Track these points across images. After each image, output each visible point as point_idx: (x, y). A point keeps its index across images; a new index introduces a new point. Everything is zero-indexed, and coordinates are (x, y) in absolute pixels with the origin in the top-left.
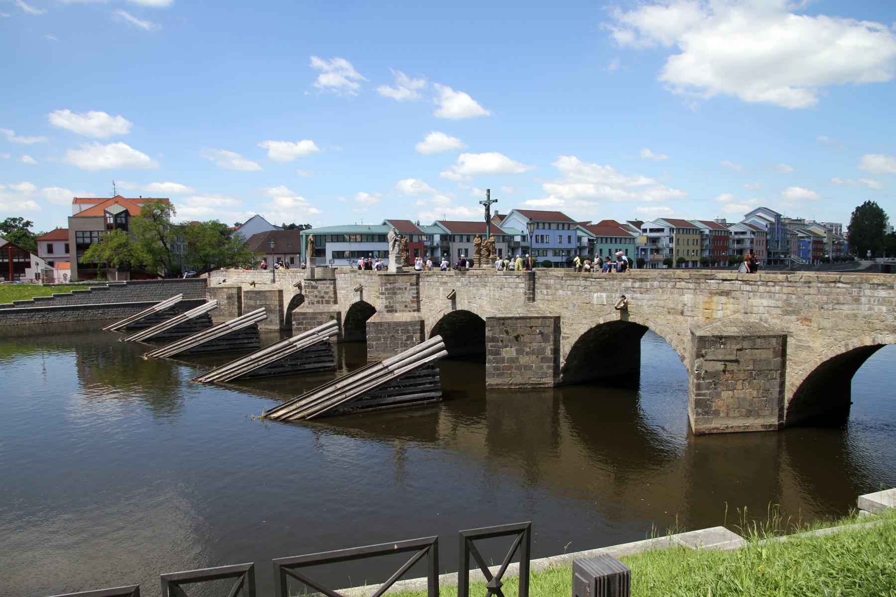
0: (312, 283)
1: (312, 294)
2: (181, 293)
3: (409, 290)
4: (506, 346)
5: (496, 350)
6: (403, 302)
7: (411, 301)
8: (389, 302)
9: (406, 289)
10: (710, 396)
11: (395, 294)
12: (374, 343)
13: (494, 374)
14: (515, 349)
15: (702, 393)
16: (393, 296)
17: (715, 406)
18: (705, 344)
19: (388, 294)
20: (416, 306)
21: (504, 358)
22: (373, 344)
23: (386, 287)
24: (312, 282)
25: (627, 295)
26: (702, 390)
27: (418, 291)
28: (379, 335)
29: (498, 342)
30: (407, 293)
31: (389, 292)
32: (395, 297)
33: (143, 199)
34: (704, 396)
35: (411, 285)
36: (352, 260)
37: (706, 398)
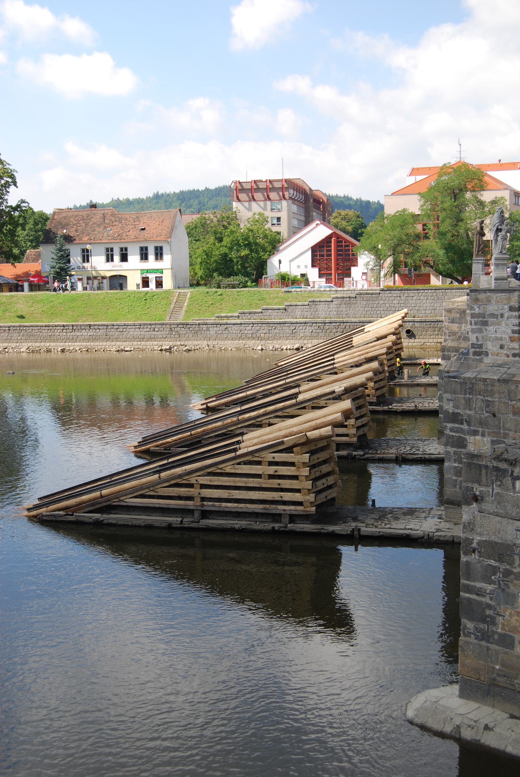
2: (406, 307)
3: (508, 318)
4: (475, 433)
5: (460, 437)
6: (497, 339)
7: (510, 338)
8: (477, 338)
9: (502, 316)
10: (491, 599)
11: (485, 324)
13: (456, 481)
14: (489, 439)
15: (475, 587)
16: (483, 328)
17: (503, 624)
18: (480, 475)
19: (476, 324)
20: (517, 347)
23: (473, 312)
26: (474, 581)
29: (462, 424)
30: (503, 323)
31: (476, 320)
32: (486, 330)
34: (477, 594)
35: (511, 309)
37: (483, 599)
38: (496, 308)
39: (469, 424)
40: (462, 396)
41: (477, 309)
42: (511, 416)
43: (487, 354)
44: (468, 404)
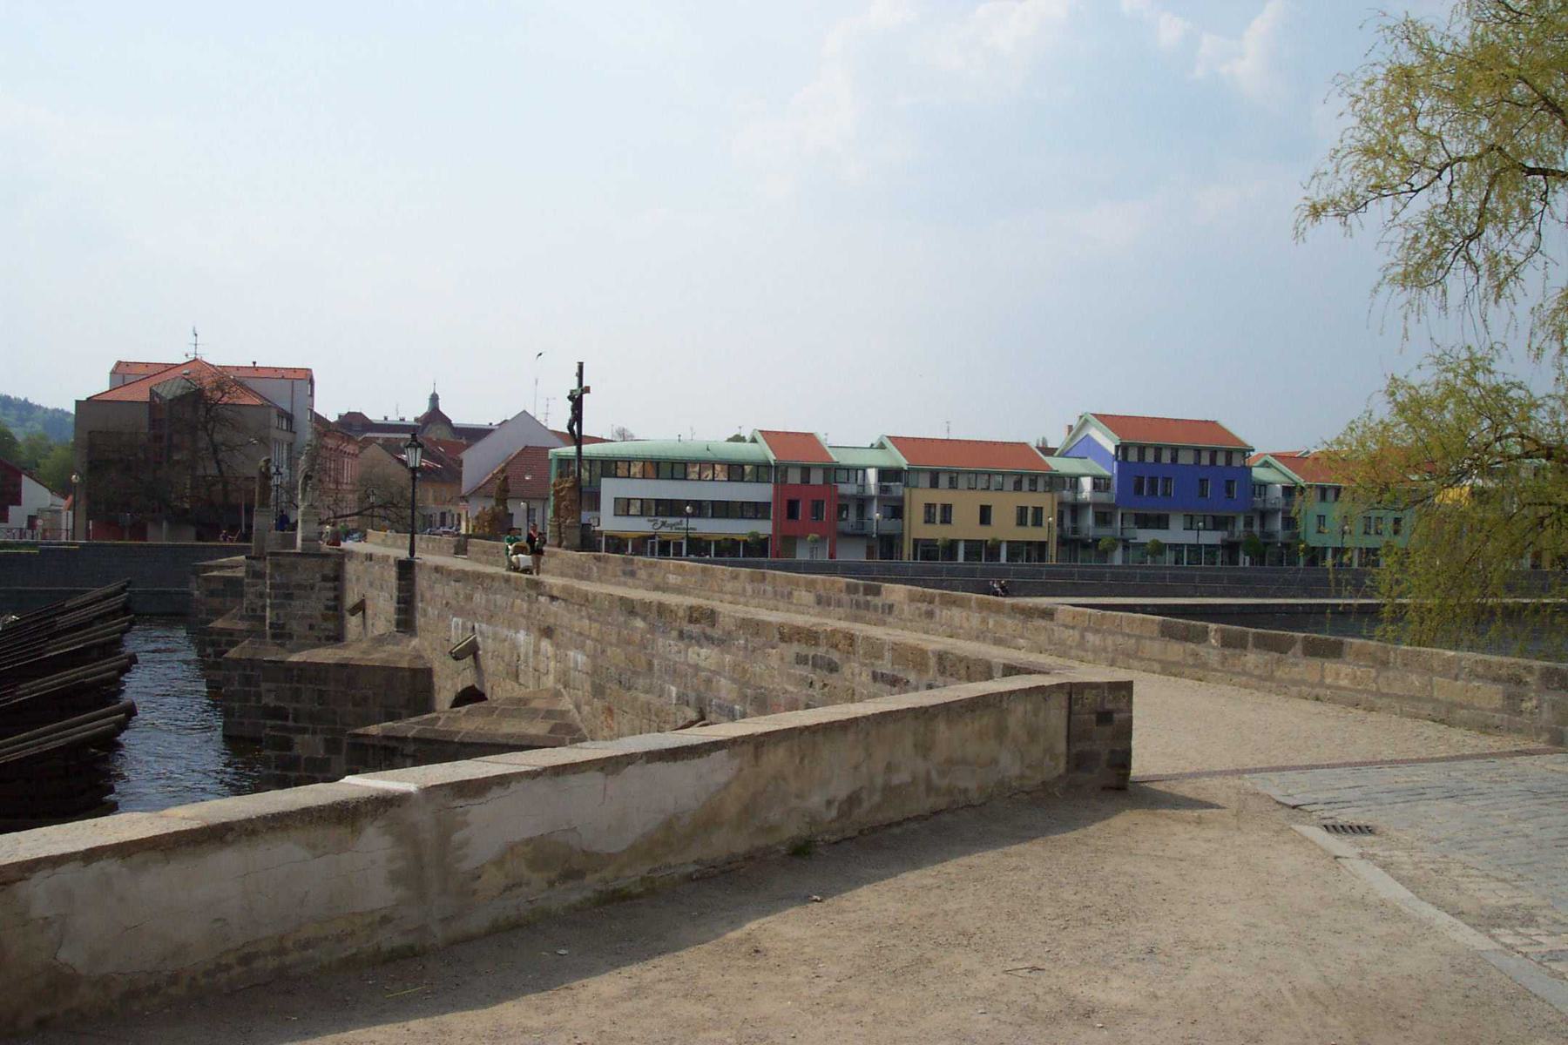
0: (254, 566)
1: (252, 590)
3: (319, 591)
4: (304, 731)
6: (304, 617)
11: (289, 596)
12: (236, 705)
19: (276, 597)
21: (298, 758)
22: (234, 709)
24: (254, 562)
25: (477, 625)
27: (336, 593)
28: (247, 689)
30: (314, 596)
32: (290, 605)
33: (257, 369)
35: (325, 578)
36: (661, 519)
38: (304, 576)
39: (295, 720)
40: (288, 686)
41: (278, 578)
42: (350, 706)
43: (290, 637)
44: (296, 696)
